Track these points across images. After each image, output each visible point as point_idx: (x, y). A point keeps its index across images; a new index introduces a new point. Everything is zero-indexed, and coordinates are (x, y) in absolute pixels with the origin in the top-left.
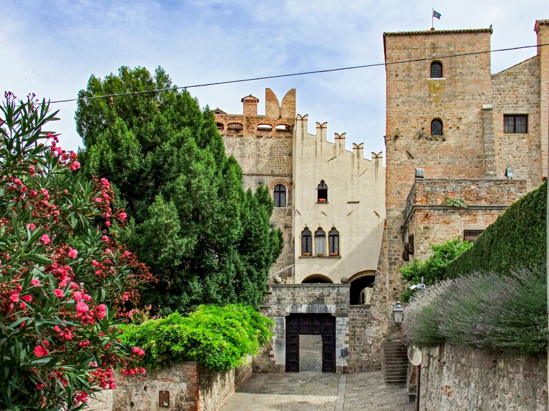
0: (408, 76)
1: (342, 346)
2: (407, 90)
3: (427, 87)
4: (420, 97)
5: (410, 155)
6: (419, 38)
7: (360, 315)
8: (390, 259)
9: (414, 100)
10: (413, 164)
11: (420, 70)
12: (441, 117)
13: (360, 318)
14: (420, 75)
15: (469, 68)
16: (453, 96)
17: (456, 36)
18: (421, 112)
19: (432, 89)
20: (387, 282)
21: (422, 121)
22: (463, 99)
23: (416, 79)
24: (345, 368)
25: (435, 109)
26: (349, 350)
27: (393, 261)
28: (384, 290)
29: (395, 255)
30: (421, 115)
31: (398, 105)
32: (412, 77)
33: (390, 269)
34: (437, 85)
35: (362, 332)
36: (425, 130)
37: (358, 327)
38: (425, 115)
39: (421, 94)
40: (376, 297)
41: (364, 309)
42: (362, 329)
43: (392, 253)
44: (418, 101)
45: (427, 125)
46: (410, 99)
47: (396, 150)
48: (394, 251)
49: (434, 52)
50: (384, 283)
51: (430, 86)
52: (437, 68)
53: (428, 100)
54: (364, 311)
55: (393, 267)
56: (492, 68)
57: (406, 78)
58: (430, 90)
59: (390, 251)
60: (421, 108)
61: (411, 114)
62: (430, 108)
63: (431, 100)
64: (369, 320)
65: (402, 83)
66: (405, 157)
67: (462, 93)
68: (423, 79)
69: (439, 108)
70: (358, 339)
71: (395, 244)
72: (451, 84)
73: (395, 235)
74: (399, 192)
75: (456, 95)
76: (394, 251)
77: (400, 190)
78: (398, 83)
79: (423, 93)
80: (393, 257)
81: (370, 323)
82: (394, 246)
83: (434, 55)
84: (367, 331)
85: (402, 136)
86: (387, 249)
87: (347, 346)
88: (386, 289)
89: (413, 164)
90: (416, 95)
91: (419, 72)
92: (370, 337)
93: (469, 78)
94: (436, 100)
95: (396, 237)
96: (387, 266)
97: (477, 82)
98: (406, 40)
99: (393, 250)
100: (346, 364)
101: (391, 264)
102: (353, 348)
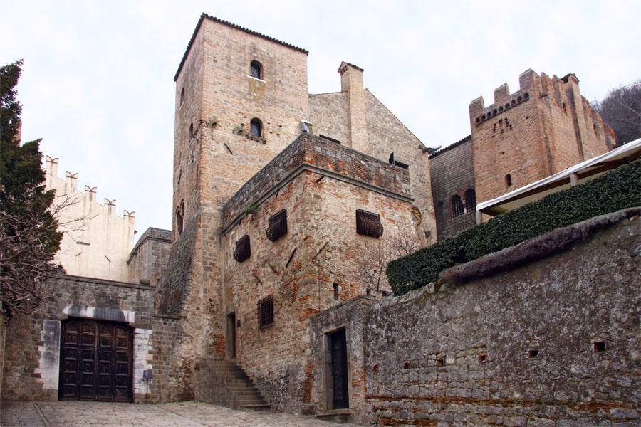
0: (227, 65)
1: (143, 366)
2: (226, 80)
3: (247, 84)
4: (239, 92)
5: (228, 148)
6: (240, 33)
7: (167, 329)
8: (205, 263)
9: (235, 93)
10: (232, 159)
11: (240, 64)
12: (261, 118)
13: (166, 331)
14: (240, 70)
15: (288, 79)
16: (273, 102)
17: (275, 45)
18: (241, 108)
19: (252, 88)
20: (202, 290)
21: (242, 116)
22: (282, 107)
23: (236, 72)
24: (147, 396)
25: (255, 108)
26: (153, 374)
27: (208, 265)
28: (197, 300)
29: (210, 259)
30: (241, 110)
31: (216, 92)
32: (232, 68)
33: (205, 275)
34: (258, 86)
35: (169, 349)
36: (245, 127)
37: (164, 343)
38: (244, 111)
39: (242, 88)
40: (188, 307)
41: (173, 321)
42: (171, 346)
43: (208, 256)
44: (237, 95)
45: (247, 121)
46: (230, 90)
47: (213, 139)
48: (210, 255)
49: (255, 52)
50: (198, 292)
51: (250, 85)
52: (256, 67)
53: (248, 97)
54: (173, 323)
55: (208, 273)
56: (309, 86)
57: (225, 67)
58: (250, 88)
59: (204, 253)
60: (241, 103)
61: (230, 105)
62: (250, 106)
63: (252, 98)
64: (179, 336)
65: (221, 71)
66: (222, 150)
67: (282, 101)
68: (242, 74)
69: (260, 109)
70: (165, 359)
71: (211, 245)
72: (271, 89)
73: (211, 235)
74: (215, 187)
75: (277, 101)
76: (210, 255)
77: (217, 184)
78: (217, 69)
79: (244, 88)
80: (208, 262)
81: (180, 339)
82: (210, 248)
83: (255, 55)
84: (176, 348)
85: (220, 126)
86: (201, 251)
87: (151, 367)
88: (199, 298)
89: (232, 159)
90: (235, 88)
91: (239, 66)
92: (180, 357)
93: (288, 89)
94: (255, 100)
95: (212, 239)
96: (202, 271)
97: (296, 96)
98: (226, 30)
99: (208, 252)
100: (149, 391)
101: (206, 269)
102: (157, 370)
